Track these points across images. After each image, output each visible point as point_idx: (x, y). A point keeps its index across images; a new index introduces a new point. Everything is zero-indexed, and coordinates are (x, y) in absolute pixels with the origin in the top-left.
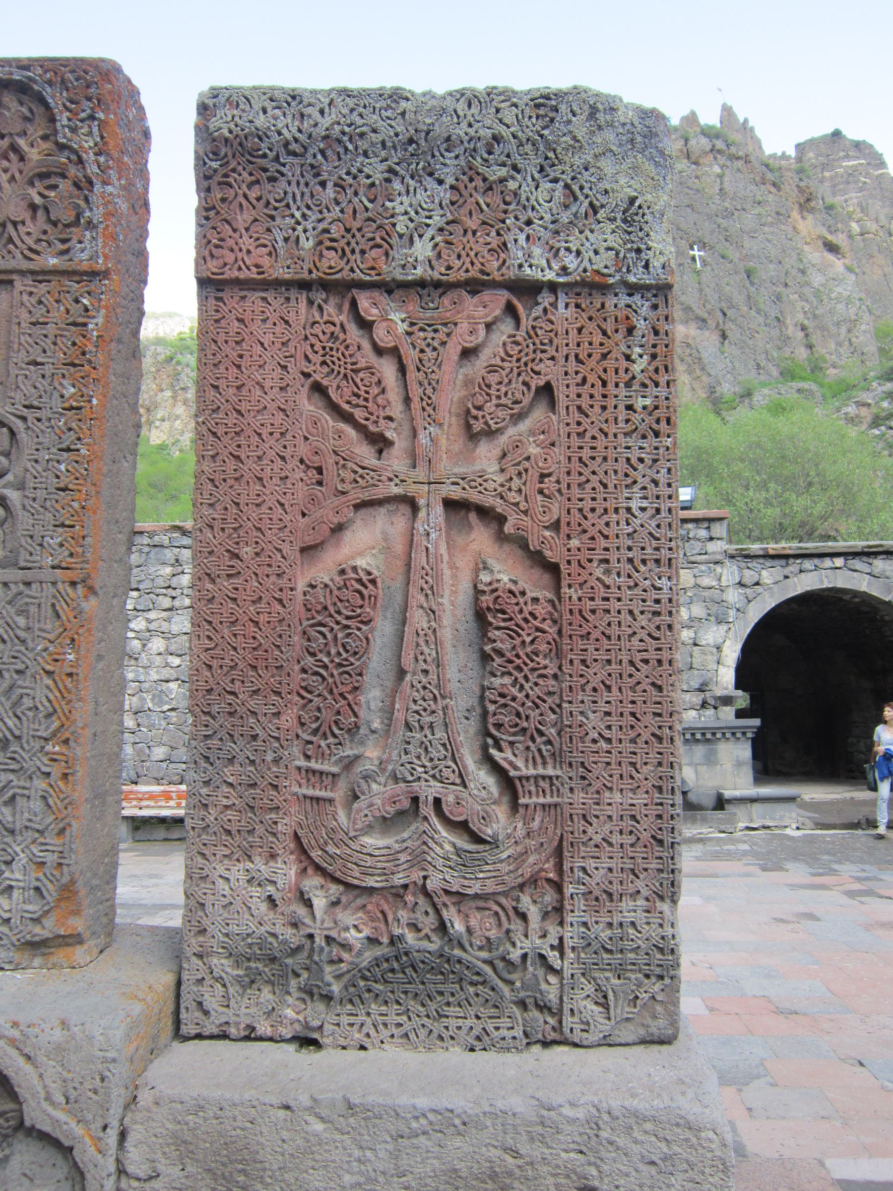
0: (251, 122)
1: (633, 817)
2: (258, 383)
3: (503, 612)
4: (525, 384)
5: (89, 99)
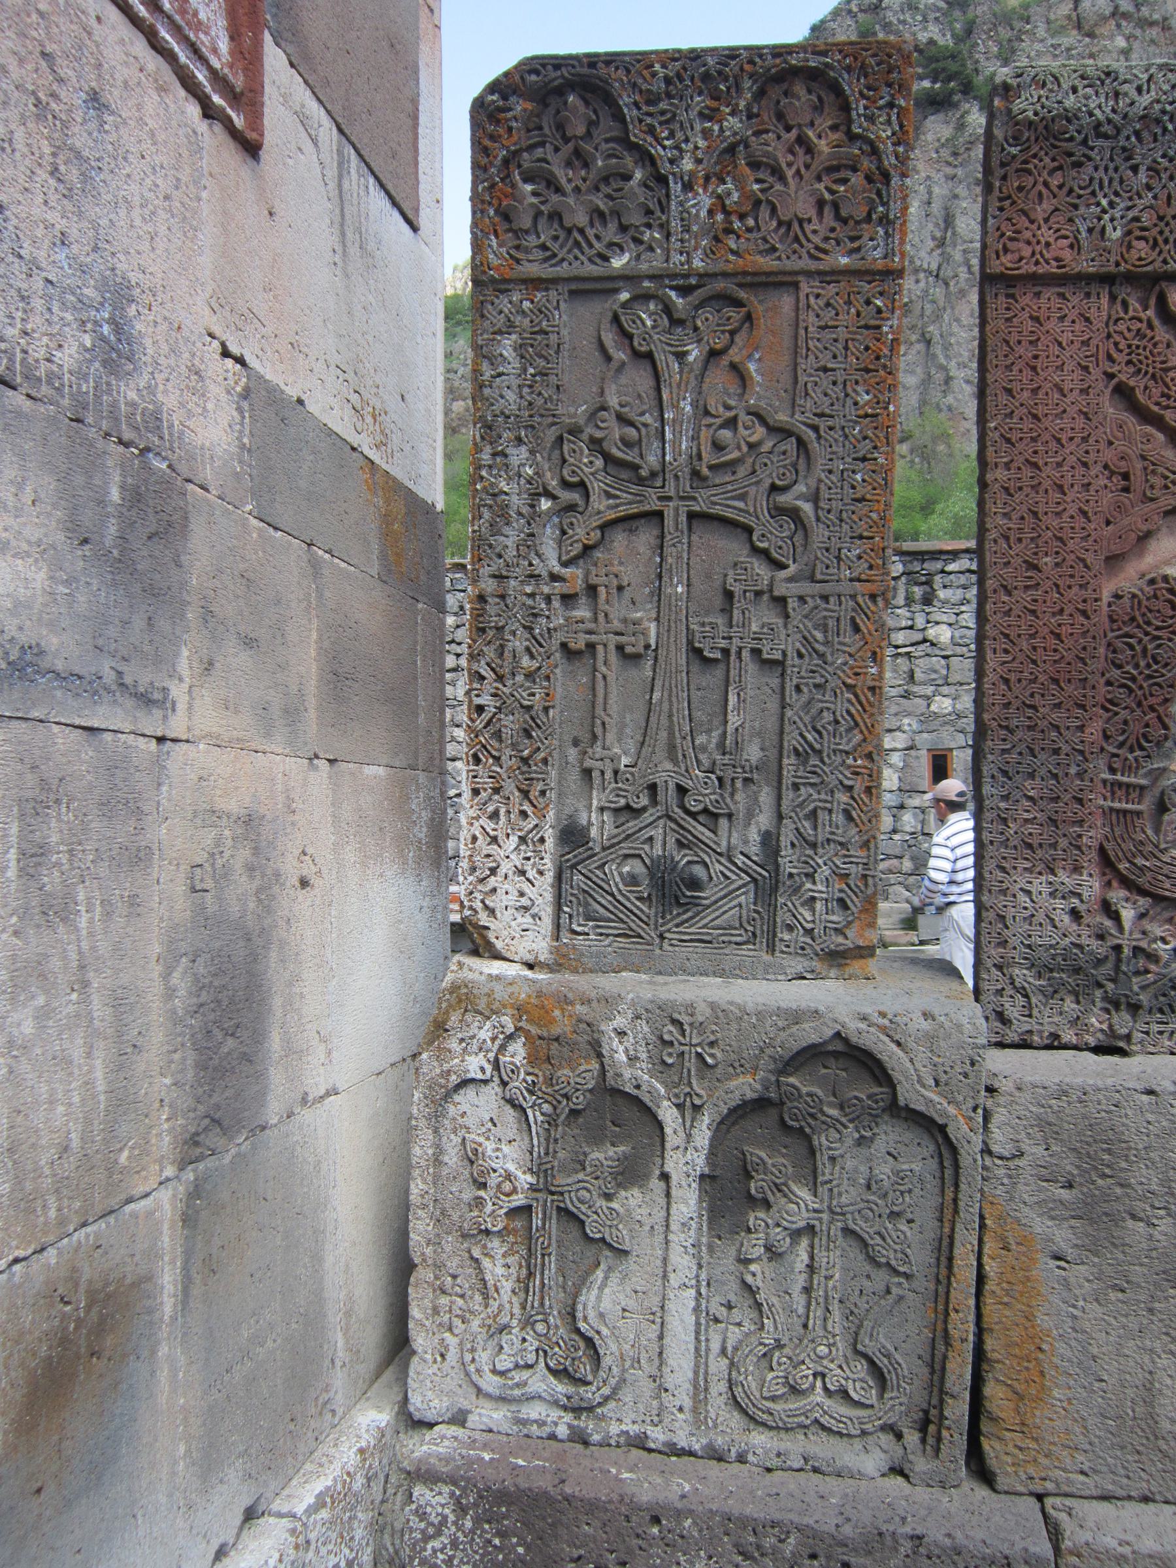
0: (1059, 102)
2: (1056, 385)
5: (889, 85)
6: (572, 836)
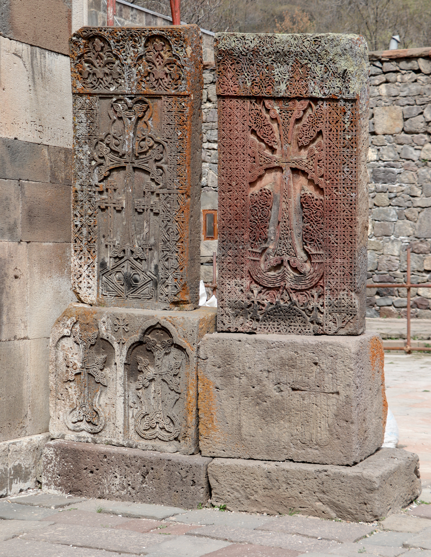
1: (344, 267)
3: (307, 203)
4: (314, 130)
6: (103, 265)
